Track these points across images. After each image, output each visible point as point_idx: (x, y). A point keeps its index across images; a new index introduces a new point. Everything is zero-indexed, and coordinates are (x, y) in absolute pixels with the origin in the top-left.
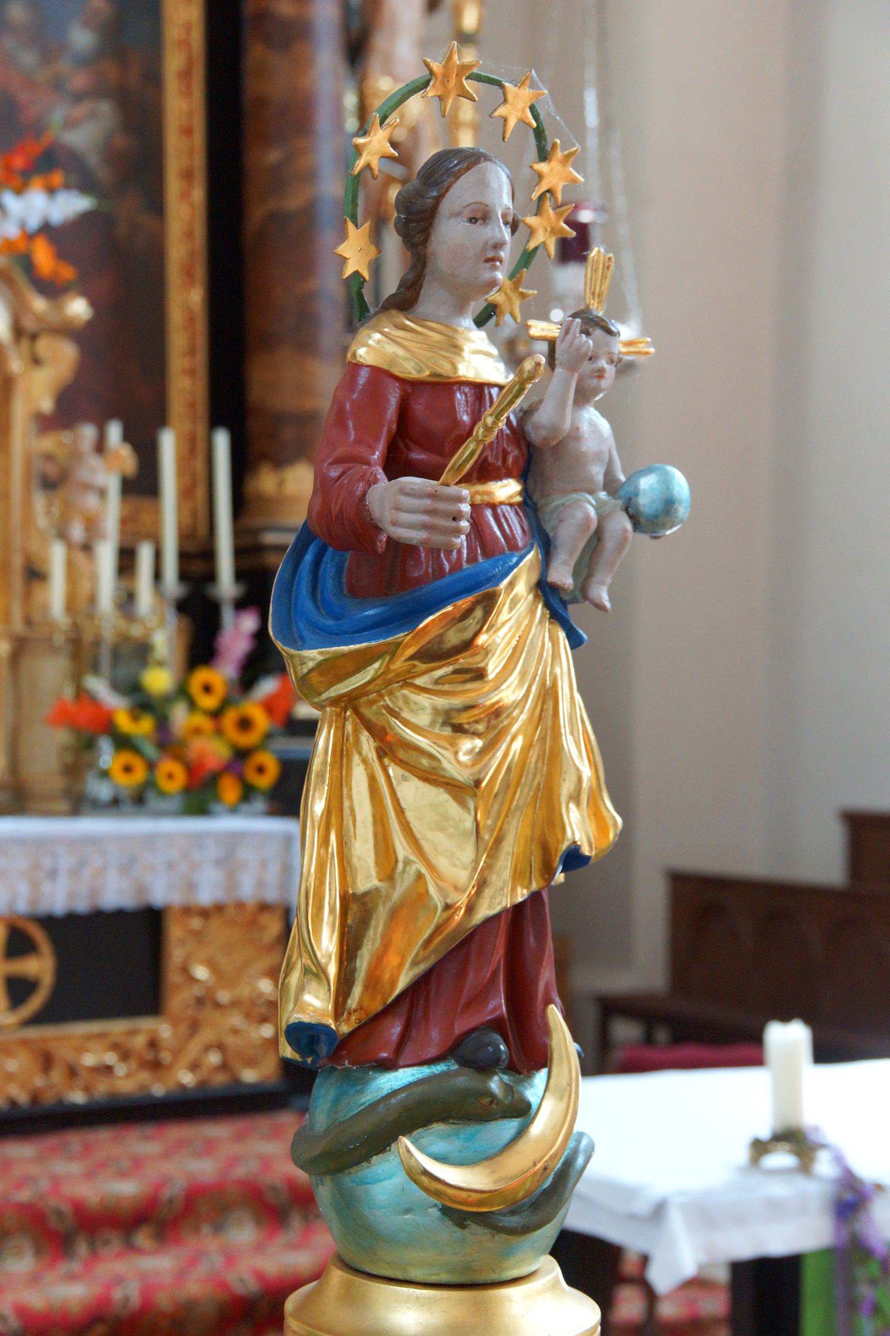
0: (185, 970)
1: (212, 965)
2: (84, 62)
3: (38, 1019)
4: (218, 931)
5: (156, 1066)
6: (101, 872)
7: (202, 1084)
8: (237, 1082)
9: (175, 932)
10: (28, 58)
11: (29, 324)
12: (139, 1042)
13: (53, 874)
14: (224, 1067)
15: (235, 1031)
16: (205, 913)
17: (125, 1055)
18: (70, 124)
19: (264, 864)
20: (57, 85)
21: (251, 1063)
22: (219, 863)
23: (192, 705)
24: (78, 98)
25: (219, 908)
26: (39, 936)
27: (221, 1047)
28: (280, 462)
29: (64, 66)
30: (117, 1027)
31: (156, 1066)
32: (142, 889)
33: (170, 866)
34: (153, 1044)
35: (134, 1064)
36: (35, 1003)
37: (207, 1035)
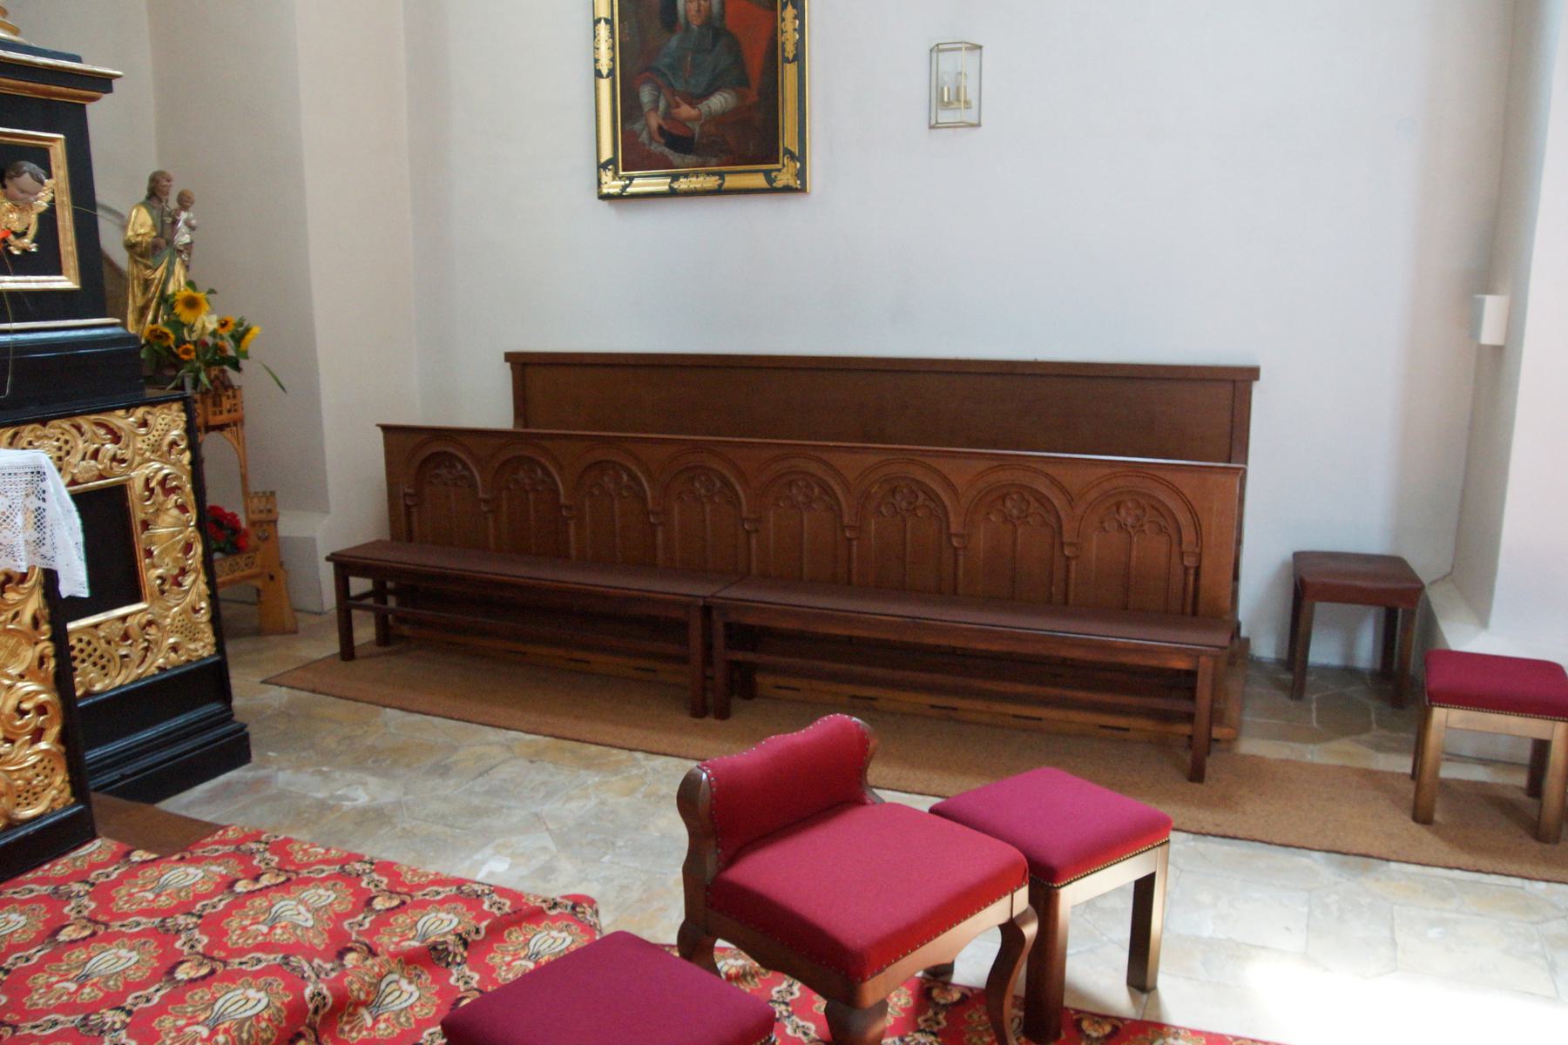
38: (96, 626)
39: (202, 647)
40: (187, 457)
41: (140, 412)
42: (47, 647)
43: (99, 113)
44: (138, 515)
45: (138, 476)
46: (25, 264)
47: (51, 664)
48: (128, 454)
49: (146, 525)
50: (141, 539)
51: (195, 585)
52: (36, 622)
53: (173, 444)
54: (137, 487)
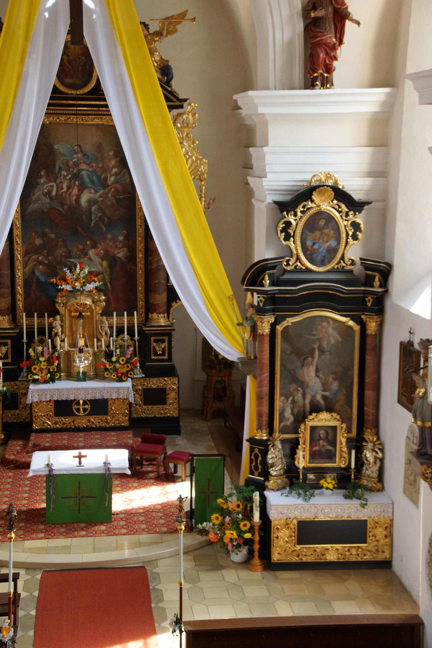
0: (111, 408)
1: (116, 407)
2: (121, 242)
3: (87, 415)
4: (117, 402)
5: (107, 422)
6: (95, 393)
7: (115, 425)
8: (121, 425)
9: (110, 402)
10: (111, 244)
11: (95, 300)
12: (104, 418)
13: (88, 394)
14: (119, 423)
15: (120, 418)
16: (114, 400)
17: (102, 421)
18: (118, 253)
19: (124, 393)
20: (116, 247)
21: (123, 422)
22: (116, 392)
23: (120, 364)
24: (120, 248)
25: (118, 399)
26: (88, 402)
27: (118, 420)
28: (152, 313)
29: (117, 244)
30: (100, 417)
31: (107, 422)
32: (103, 396)
33: (108, 392)
34: (106, 419)
35: (103, 422)
36: (87, 412)
37: (115, 418)
38: (158, 407)
39: (176, 415)
40: (177, 385)
41: (170, 378)
42: (128, 407)
43: (174, 333)
44: (168, 392)
45: (168, 387)
46: (160, 355)
47: (129, 409)
48: (167, 383)
49: (168, 394)
50: (167, 396)
51: (176, 405)
52: (127, 404)
53: (175, 383)
54: (168, 389)
